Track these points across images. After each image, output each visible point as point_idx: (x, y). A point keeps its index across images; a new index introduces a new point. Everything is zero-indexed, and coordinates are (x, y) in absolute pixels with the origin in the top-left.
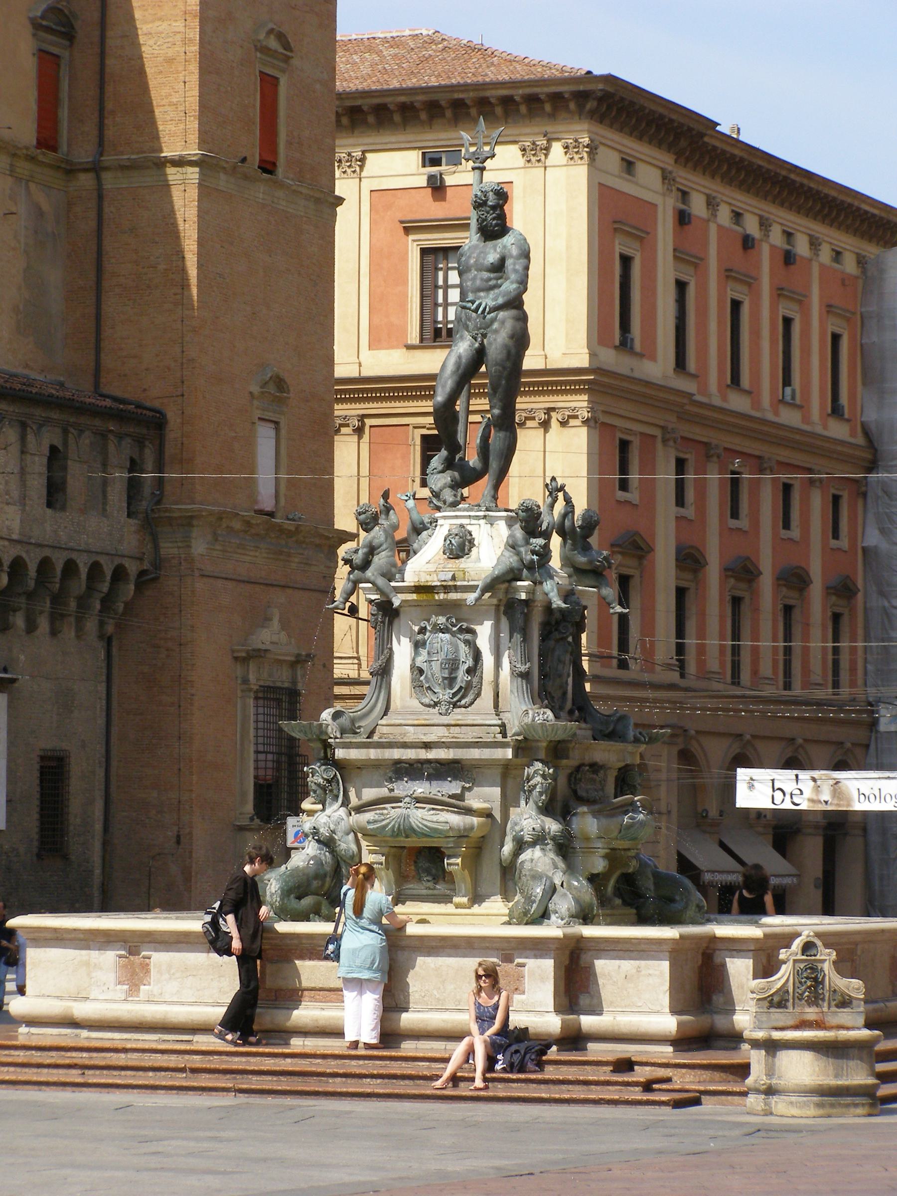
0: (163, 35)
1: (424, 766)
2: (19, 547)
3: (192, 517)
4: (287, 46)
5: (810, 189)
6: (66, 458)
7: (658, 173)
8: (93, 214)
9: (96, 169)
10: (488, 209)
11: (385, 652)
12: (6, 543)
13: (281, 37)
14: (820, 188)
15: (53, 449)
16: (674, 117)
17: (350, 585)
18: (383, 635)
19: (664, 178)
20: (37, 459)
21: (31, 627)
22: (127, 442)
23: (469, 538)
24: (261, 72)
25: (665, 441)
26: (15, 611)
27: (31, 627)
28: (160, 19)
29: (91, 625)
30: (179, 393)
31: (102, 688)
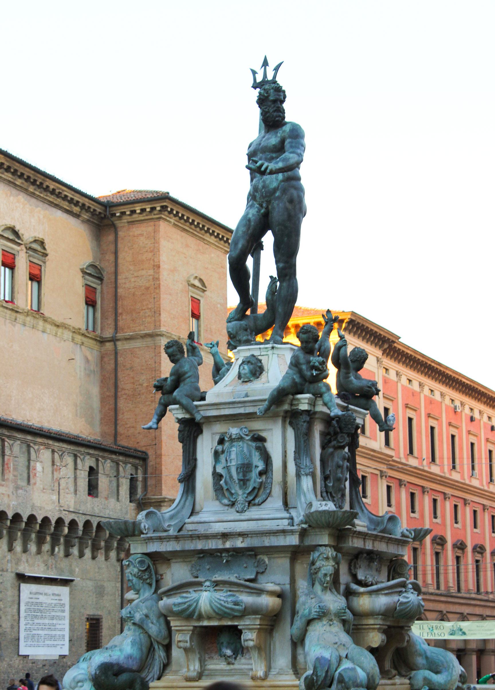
0: (144, 277)
1: (223, 555)
2: (73, 515)
3: (161, 502)
4: (203, 284)
5: (440, 370)
6: (97, 473)
7: (375, 359)
8: (113, 362)
9: (114, 340)
10: (270, 103)
11: (191, 462)
12: (67, 512)
13: (201, 280)
14: (445, 370)
15: (91, 468)
16: (382, 333)
17: (162, 407)
18: (189, 448)
19: (378, 361)
20: (82, 472)
21: (81, 555)
22: (129, 465)
23: (260, 364)
24: (191, 296)
25: (381, 477)
26: (72, 546)
27: (81, 555)
28: (143, 269)
29: (113, 554)
30: (154, 443)
31: (119, 585)
